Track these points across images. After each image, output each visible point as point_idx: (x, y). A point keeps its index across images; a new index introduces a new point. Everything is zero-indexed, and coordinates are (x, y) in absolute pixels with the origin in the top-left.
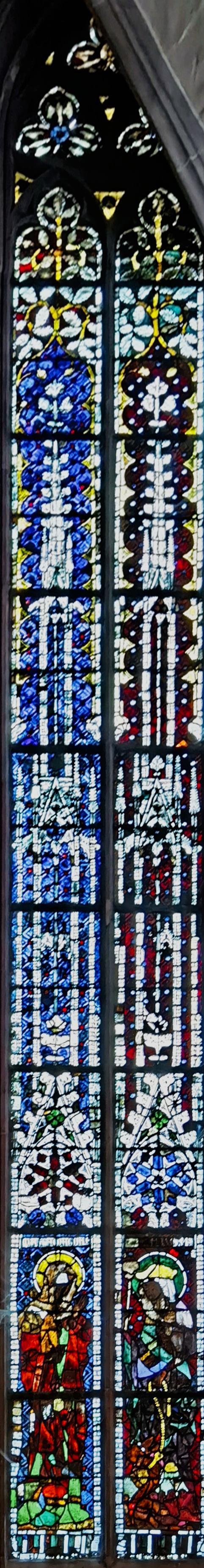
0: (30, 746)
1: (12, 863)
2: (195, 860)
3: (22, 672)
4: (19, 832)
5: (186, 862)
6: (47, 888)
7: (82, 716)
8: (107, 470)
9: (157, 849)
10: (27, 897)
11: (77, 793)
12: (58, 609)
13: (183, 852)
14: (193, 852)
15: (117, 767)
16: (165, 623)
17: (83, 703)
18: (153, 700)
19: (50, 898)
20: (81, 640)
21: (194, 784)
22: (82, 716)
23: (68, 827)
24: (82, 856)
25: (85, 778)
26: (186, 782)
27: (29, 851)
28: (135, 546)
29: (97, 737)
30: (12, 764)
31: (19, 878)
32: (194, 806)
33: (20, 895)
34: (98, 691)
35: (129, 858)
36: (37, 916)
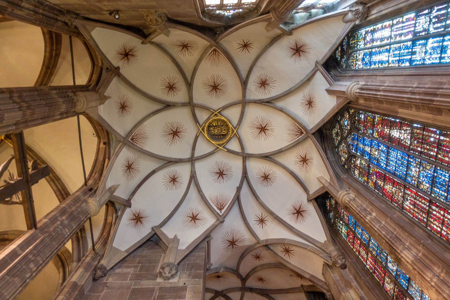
0: (411, 61)
1: (431, 64)
2: (437, 8)
3: (399, 63)
4: (425, 62)
5: (438, 10)
6: (437, 53)
7: (407, 48)
8: (375, 47)
9: (434, 20)
10: (438, 59)
11: (420, 46)
12: (391, 56)
13: (436, 12)
14: (436, 8)
15: (417, 36)
16: (396, 28)
17: (405, 47)
18: (407, 28)
19: (439, 52)
20: (396, 49)
21: (422, 13)
22: (407, 48)
23: (426, 49)
24: (432, 43)
25: (418, 45)
26: (421, 15)
27: (429, 59)
28: (385, 38)
29: (411, 42)
30: (413, 65)
31: (434, 62)
32: (426, 12)
33: (437, 61)
34: (404, 44)
35: (435, 29)
36: (443, 55)
